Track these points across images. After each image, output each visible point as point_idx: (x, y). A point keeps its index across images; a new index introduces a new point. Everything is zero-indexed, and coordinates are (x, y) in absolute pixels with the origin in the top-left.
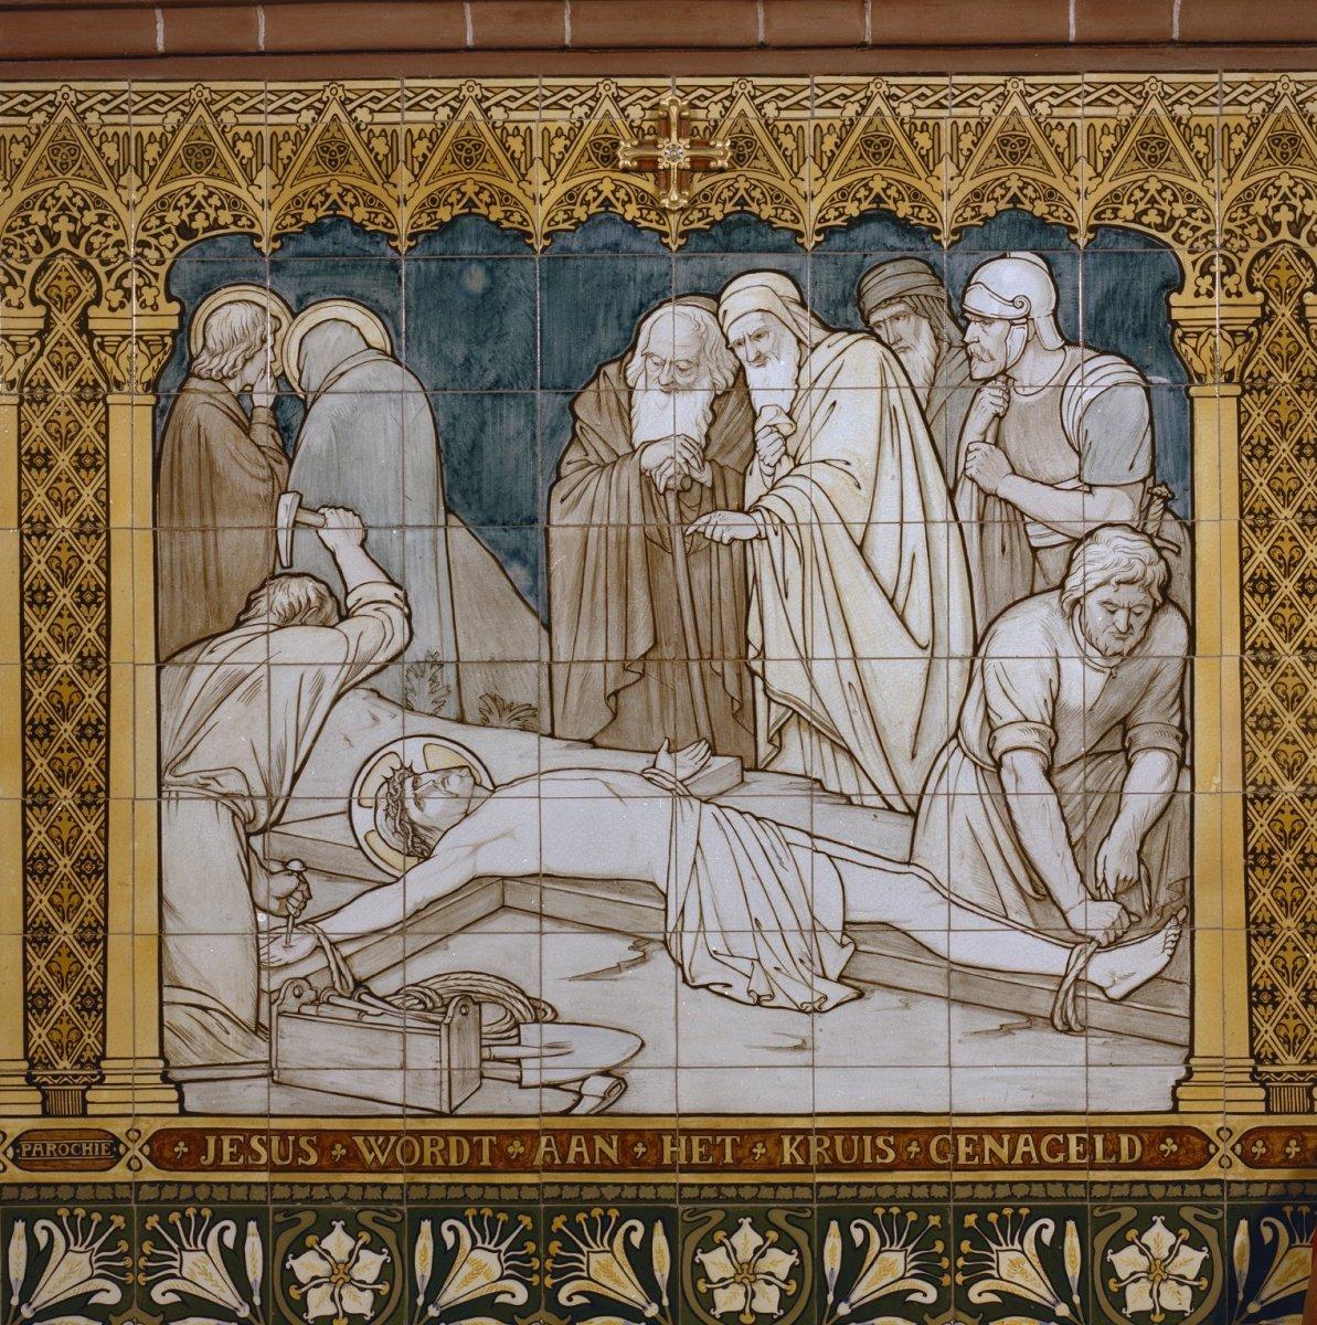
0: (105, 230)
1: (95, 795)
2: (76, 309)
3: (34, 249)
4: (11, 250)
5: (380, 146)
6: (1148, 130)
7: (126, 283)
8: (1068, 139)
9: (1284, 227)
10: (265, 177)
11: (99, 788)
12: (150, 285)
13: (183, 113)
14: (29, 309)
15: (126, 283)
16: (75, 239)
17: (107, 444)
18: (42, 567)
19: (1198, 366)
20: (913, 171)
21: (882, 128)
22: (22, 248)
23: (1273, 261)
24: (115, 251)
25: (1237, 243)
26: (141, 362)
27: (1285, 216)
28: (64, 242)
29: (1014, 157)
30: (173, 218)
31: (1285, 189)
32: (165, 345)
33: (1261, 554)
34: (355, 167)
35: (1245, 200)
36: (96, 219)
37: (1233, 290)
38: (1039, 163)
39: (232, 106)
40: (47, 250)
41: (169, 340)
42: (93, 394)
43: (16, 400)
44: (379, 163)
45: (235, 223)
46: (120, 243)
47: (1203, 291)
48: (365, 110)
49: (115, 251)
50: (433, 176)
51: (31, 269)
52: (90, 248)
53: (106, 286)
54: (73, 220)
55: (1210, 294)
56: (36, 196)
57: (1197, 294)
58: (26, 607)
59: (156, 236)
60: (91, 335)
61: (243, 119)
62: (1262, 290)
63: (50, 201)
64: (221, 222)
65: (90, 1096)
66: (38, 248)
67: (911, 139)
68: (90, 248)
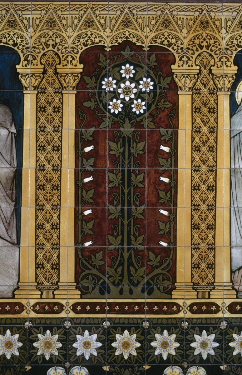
0: (23, 44)
1: (57, 206)
2: (53, 68)
3: (42, 49)
4: (35, 49)
5: (102, 21)
6: (88, 17)
7: (28, 59)
8: (182, 22)
9: (204, 47)
10: (31, 30)
11: (58, 204)
12: (229, 61)
13: (85, 11)
14: (40, 66)
15: (28, 59)
16: (207, 47)
17: (62, 105)
18: (198, 140)
19: (219, 86)
20: (99, 30)
21: (13, 17)
22: (38, 49)
23: (209, 58)
24: (65, 50)
25: (76, 51)
26: (33, 81)
27: (204, 44)
28: (51, 48)
29: (12, 26)
30: (197, 41)
31: (204, 37)
32: (41, 76)
33: (197, 139)
34: (18, 27)
35: (193, 40)
36: (213, 42)
37: (190, 65)
38: (96, 28)
39: (99, 9)
40: (46, 50)
41: (79, 75)
42: (59, 91)
43: (191, 93)
44: (64, 26)
45: (100, 42)
46: (28, 48)
47: (180, 65)
48: (60, 11)
49: (219, 51)
50: (117, 30)
51: (40, 55)
52: (212, 51)
53: (217, 60)
54: (207, 42)
55: (182, 66)
56: (196, 36)
57: (63, 66)
58: (38, 151)
59: (38, 45)
60: (213, 74)
61: (102, 12)
62: (199, 65)
63: (47, 35)
64: (96, 42)
65: (55, 293)
66: (43, 49)
67: (214, 23)
68: (58, 50)
